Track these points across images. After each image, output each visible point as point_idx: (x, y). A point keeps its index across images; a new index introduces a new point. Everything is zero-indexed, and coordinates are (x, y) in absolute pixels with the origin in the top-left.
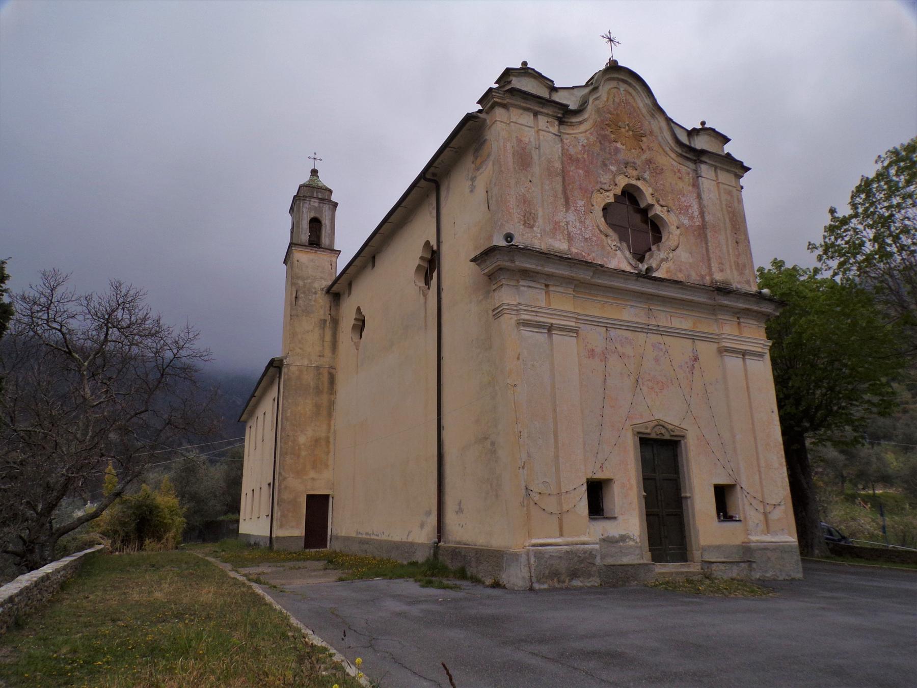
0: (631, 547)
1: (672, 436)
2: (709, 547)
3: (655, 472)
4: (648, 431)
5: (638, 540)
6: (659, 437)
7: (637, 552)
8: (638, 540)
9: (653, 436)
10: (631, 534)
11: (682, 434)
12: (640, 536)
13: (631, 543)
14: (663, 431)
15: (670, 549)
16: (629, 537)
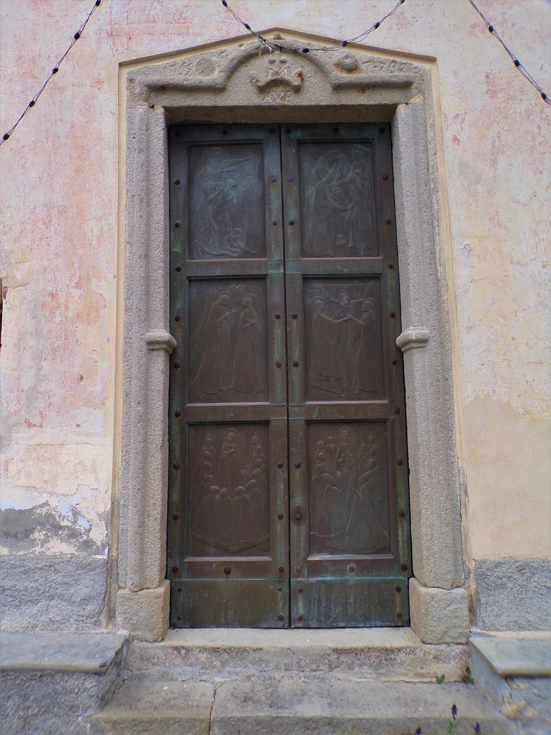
0: (52, 565)
1: (339, 88)
2: (524, 567)
3: (264, 251)
4: (215, 76)
5: (98, 535)
6: (273, 99)
7: (89, 585)
8: (98, 535)
9: (241, 95)
10: (61, 508)
11: (399, 76)
12: (112, 517)
13: (58, 547)
14: (290, 69)
15: (316, 568)
16: (51, 525)
